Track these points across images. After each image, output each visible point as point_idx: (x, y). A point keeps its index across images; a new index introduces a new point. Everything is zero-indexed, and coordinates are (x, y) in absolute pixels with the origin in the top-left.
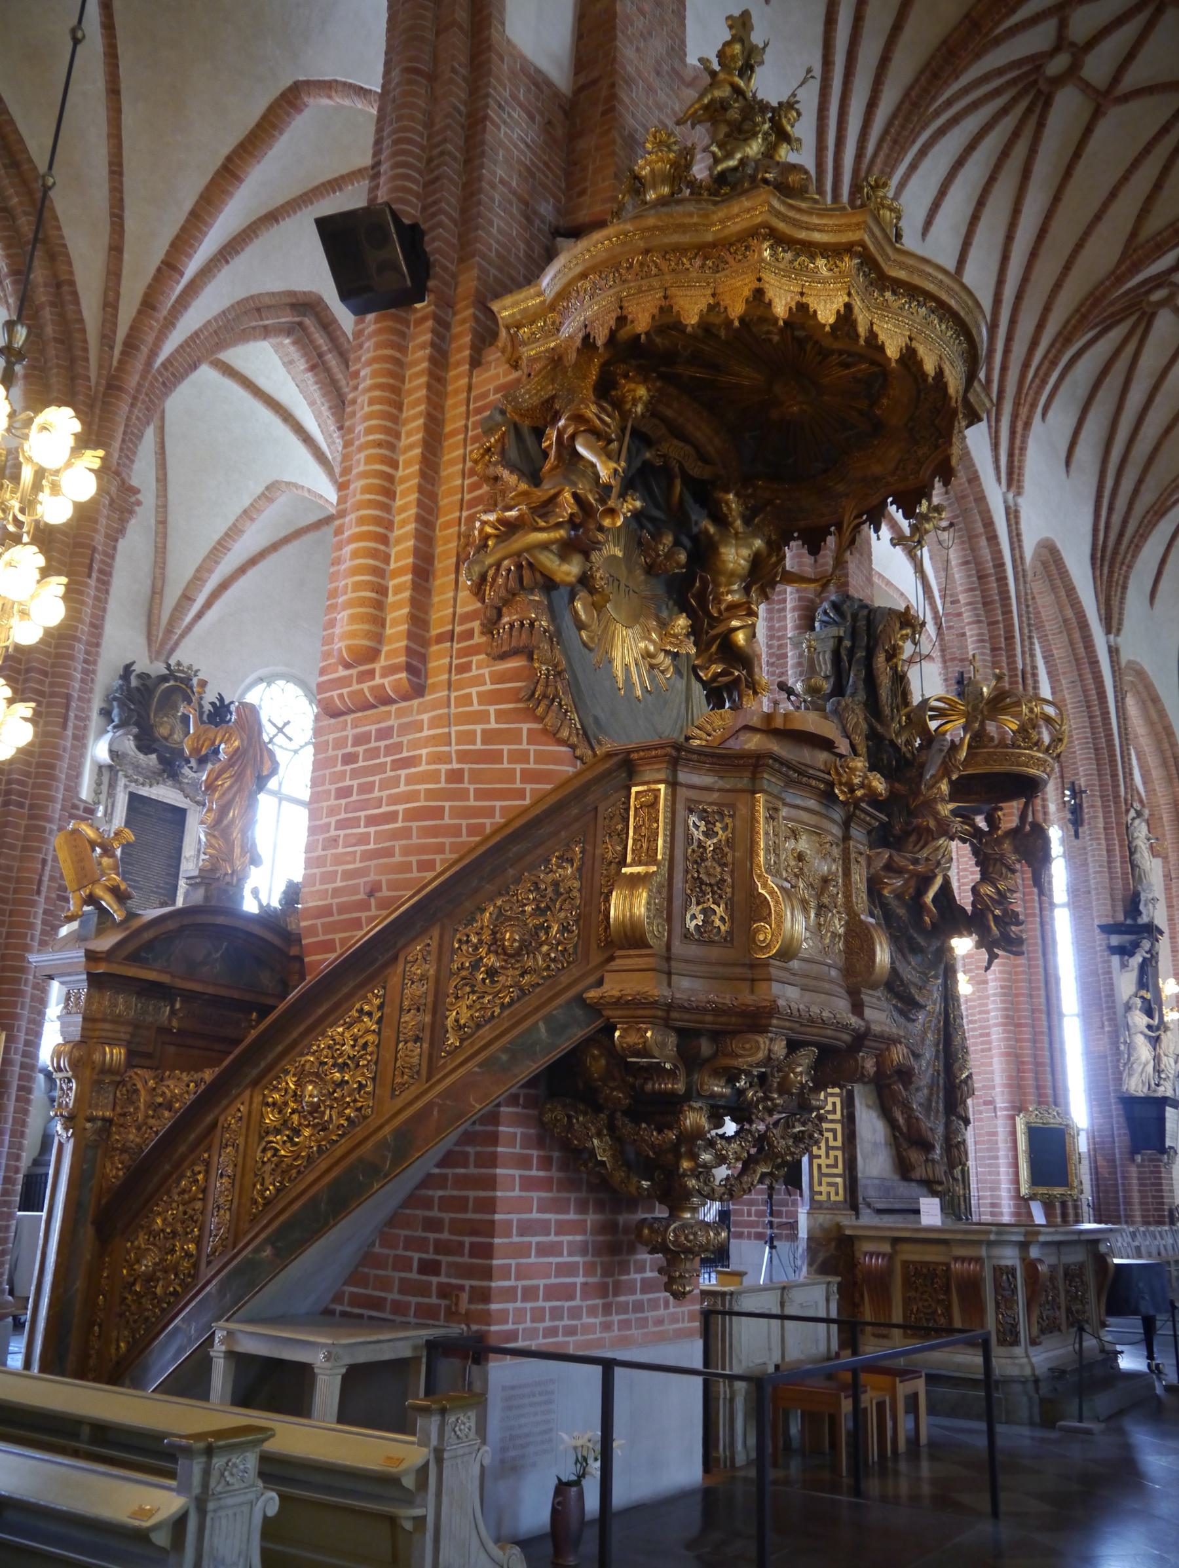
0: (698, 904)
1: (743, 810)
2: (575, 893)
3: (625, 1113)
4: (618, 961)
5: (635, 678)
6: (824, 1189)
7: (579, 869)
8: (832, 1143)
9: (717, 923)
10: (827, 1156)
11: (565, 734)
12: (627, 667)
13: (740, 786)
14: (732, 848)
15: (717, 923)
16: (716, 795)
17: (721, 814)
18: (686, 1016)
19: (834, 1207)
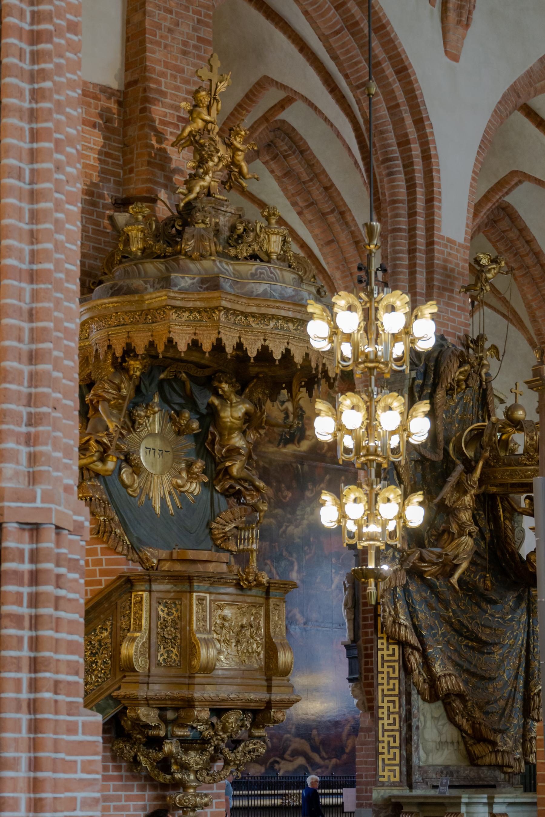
0: (164, 648)
1: (186, 602)
2: (109, 645)
3: (144, 745)
4: (127, 678)
5: (169, 503)
6: (386, 774)
7: (110, 633)
8: (392, 744)
9: (174, 657)
10: (389, 752)
11: (120, 549)
12: (163, 500)
13: (184, 589)
14: (181, 621)
15: (174, 657)
16: (172, 594)
17: (175, 603)
18: (158, 702)
19: (393, 785)
